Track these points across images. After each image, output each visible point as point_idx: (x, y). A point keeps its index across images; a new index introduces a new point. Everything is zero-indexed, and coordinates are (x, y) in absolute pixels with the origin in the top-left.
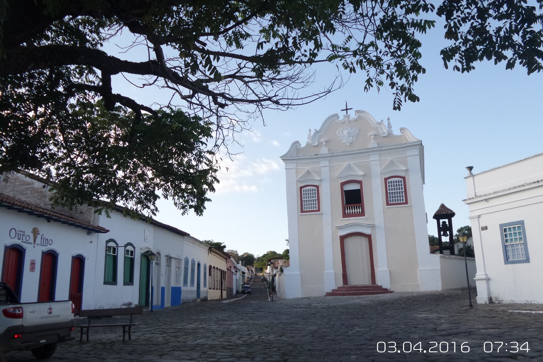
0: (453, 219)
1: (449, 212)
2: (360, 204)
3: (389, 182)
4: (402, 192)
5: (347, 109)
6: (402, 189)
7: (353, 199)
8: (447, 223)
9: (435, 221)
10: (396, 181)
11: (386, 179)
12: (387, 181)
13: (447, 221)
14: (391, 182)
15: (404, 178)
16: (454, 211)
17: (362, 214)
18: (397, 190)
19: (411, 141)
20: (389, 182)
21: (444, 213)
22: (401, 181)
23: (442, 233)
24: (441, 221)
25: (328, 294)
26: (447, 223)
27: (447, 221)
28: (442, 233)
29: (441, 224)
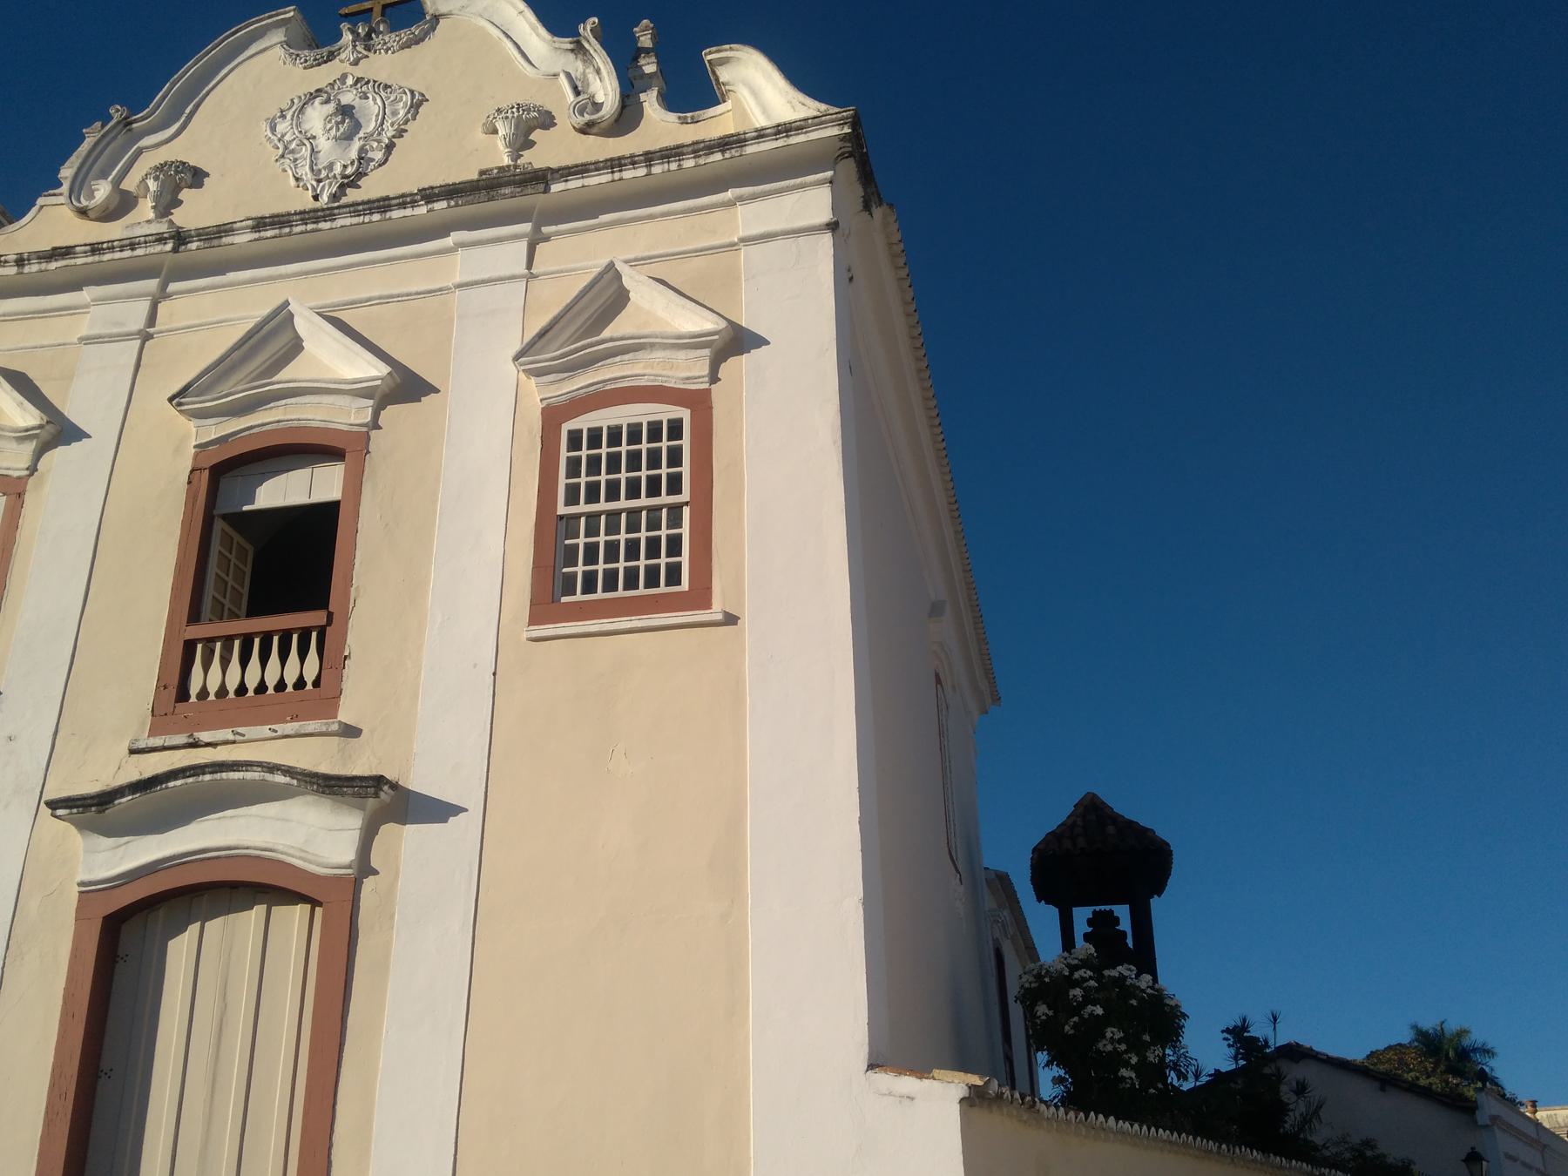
2: (314, 618)
4: (675, 511)
8: (1125, 925)
9: (1052, 912)
11: (553, 416)
13: (1122, 912)
15: (699, 402)
17: (318, 696)
19: (761, 121)
20: (575, 440)
22: (676, 429)
26: (1125, 925)
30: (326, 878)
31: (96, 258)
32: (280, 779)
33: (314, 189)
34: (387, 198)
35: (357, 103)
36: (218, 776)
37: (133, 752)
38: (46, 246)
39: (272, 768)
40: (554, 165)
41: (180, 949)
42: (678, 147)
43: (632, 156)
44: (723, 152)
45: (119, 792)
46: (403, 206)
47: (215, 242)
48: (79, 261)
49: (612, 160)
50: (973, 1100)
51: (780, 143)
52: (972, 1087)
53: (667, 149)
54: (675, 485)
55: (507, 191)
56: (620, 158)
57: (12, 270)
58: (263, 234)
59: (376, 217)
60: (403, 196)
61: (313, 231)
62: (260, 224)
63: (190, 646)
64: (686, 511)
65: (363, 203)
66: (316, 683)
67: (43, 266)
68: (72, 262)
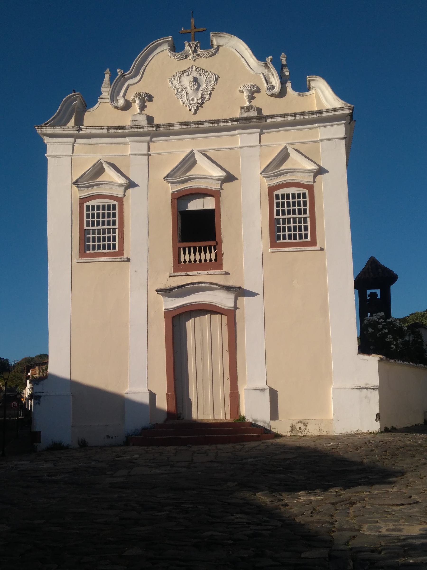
0: (394, 289)
2: (212, 243)
4: (305, 219)
6: (305, 213)
7: (197, 229)
10: (293, 195)
11: (271, 189)
13: (378, 292)
14: (283, 196)
15: (310, 188)
16: (396, 272)
17: (217, 264)
18: (294, 213)
19: (329, 107)
20: (277, 196)
26: (379, 297)
27: (378, 292)
30: (227, 309)
31: (132, 130)
32: (215, 286)
33: (189, 107)
34: (220, 120)
35: (198, 76)
36: (199, 285)
37: (170, 276)
38: (117, 125)
39: (213, 284)
40: (268, 114)
41: (190, 324)
42: (304, 112)
43: (291, 114)
44: (316, 115)
45: (175, 288)
46: (224, 122)
47: (168, 128)
48: (127, 131)
49: (285, 114)
50: (380, 360)
51: (332, 114)
52: (381, 358)
53: (301, 112)
54: (305, 212)
55: (255, 120)
56: (287, 114)
57: (106, 131)
58: (183, 127)
59: (216, 125)
60: (224, 119)
61: (198, 127)
62: (182, 124)
63: (179, 248)
64: (308, 219)
65: (212, 120)
66: (216, 260)
67: (116, 131)
68: (125, 131)
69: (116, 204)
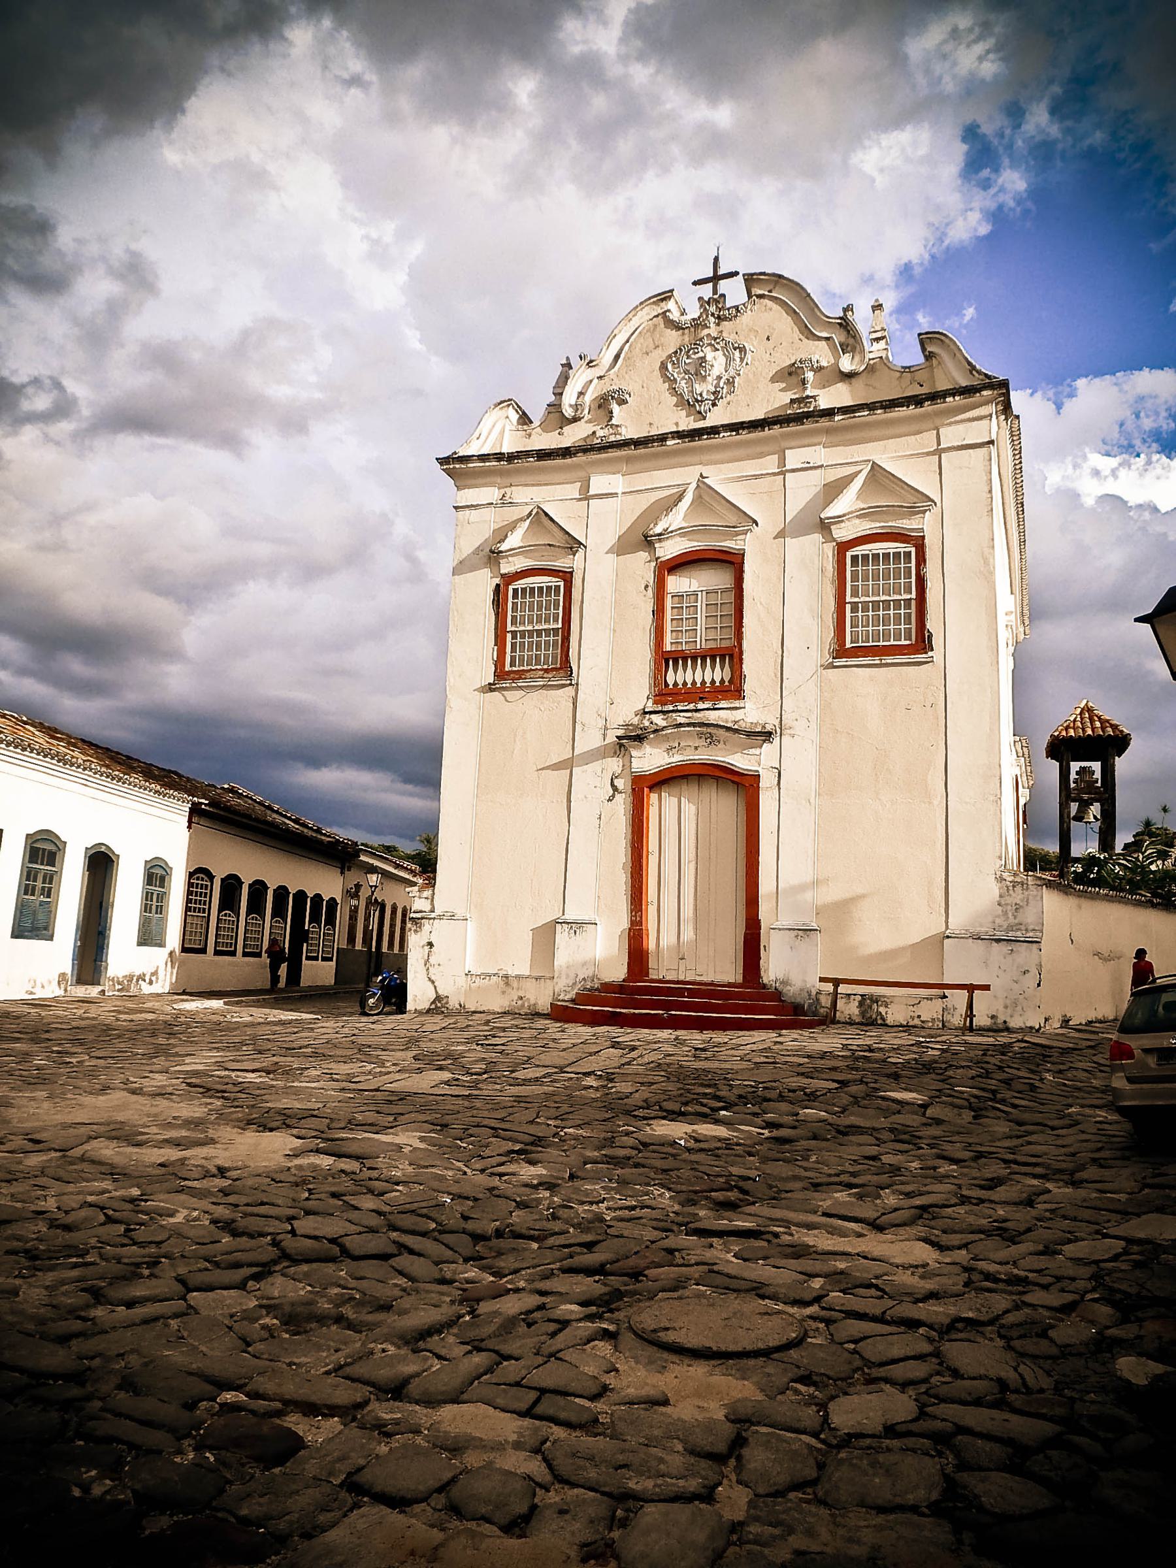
1: (1110, 731)
3: (855, 559)
5: (716, 278)
12: (849, 554)
13: (1096, 766)
14: (865, 557)
17: (734, 689)
20: (855, 559)
21: (1089, 732)
23: (1074, 807)
24: (1075, 766)
25: (562, 1013)
26: (1098, 775)
27: (1096, 766)
28: (1074, 807)
29: (1073, 776)
69: (562, 584)
